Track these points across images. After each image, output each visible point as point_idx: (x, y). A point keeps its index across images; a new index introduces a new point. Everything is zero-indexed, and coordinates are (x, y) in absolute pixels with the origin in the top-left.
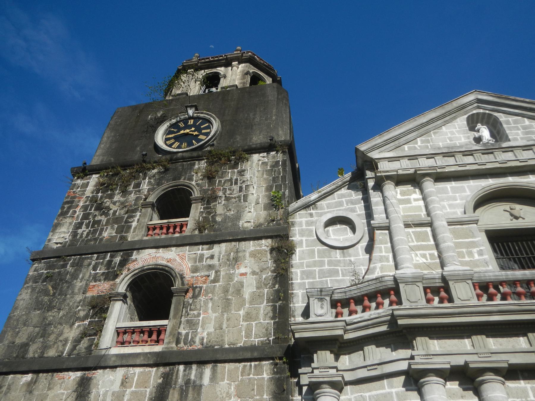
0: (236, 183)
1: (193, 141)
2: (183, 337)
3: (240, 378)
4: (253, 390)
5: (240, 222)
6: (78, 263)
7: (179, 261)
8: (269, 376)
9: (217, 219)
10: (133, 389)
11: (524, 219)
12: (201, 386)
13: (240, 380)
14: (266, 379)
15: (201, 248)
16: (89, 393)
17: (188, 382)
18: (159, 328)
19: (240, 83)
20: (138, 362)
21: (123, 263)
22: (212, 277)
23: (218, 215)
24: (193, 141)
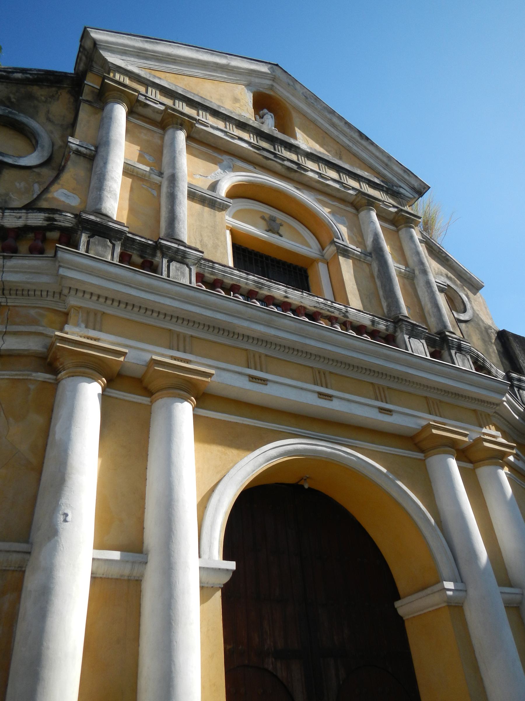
11: (281, 236)
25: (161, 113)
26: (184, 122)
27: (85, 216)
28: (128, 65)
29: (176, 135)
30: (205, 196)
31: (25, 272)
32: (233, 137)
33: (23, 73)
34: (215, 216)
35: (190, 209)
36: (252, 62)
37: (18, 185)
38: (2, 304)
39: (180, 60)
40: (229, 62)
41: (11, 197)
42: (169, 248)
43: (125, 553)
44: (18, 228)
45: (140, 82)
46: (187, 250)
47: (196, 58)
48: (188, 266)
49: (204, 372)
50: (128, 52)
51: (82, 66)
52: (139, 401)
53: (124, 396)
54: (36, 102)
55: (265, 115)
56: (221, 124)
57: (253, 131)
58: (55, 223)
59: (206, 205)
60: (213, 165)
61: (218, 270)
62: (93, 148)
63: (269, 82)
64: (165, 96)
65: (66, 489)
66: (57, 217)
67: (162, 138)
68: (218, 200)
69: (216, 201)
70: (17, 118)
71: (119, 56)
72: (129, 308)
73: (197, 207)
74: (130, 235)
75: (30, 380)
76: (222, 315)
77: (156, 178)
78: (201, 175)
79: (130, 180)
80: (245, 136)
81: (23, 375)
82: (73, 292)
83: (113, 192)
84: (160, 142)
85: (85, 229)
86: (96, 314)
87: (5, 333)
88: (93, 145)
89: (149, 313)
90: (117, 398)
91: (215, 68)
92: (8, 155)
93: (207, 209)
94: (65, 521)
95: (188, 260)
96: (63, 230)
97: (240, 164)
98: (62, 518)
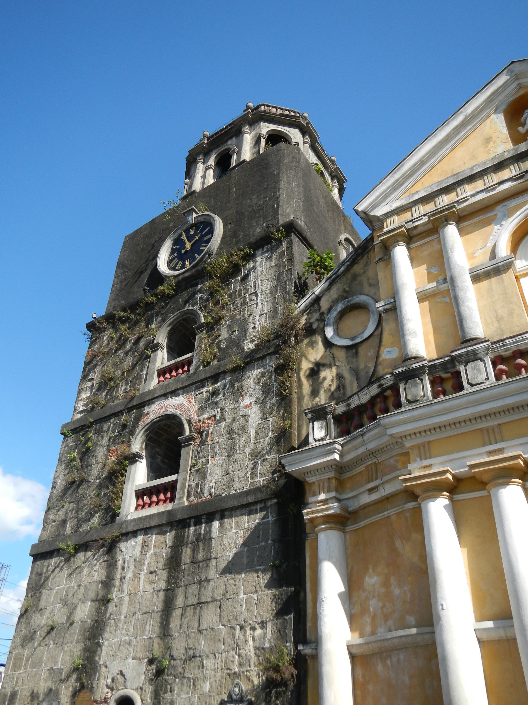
0: (240, 295)
1: (196, 255)
2: (194, 490)
3: (246, 524)
4: (259, 537)
5: (245, 342)
6: (99, 430)
7: (187, 405)
8: (274, 519)
9: (222, 346)
10: (152, 551)
12: (211, 539)
13: (246, 527)
14: (271, 522)
15: (206, 385)
16: (116, 562)
17: (198, 538)
18: (172, 484)
19: (254, 154)
20: (154, 523)
21: (137, 419)
22: (218, 416)
23: (222, 341)
24: (196, 255)
25: (429, 223)
26: (447, 216)
27: (396, 372)
28: (392, 205)
29: (445, 234)
30: (488, 270)
31: (375, 439)
32: (493, 187)
33: (344, 265)
34: (503, 281)
35: (478, 293)
36: (486, 89)
37: (369, 354)
38: (377, 462)
39: (427, 158)
40: (465, 113)
41: (369, 367)
42: (460, 355)
43: (496, 621)
44: (369, 401)
45: (405, 210)
46: (475, 347)
47: (436, 143)
48: (481, 360)
49: (512, 456)
50: (387, 195)
51: (371, 227)
52: (481, 495)
53: (467, 496)
54: (359, 278)
55: (526, 119)
56: (479, 185)
57: (512, 161)
58: (384, 386)
59: (492, 276)
60: (487, 229)
61: (510, 344)
62: (392, 300)
63: (514, 85)
64: (427, 204)
65: (438, 586)
66: (382, 382)
67: (439, 241)
68: (500, 264)
69: (498, 267)
70: (353, 302)
71: (384, 204)
72: (443, 429)
73: (485, 284)
74: (431, 363)
75: (405, 510)
76: (514, 397)
77: (444, 287)
78: (480, 249)
79: (427, 303)
80: (506, 174)
81: (401, 508)
82: (404, 439)
83: (412, 333)
84: (439, 246)
85: (401, 380)
86: (424, 446)
87: (383, 484)
88: (391, 298)
89: (458, 425)
90: (463, 500)
91: (457, 132)
92: (356, 336)
93: (494, 280)
94: (443, 609)
95: (479, 355)
96: (390, 387)
97: (513, 203)
98: (440, 608)
